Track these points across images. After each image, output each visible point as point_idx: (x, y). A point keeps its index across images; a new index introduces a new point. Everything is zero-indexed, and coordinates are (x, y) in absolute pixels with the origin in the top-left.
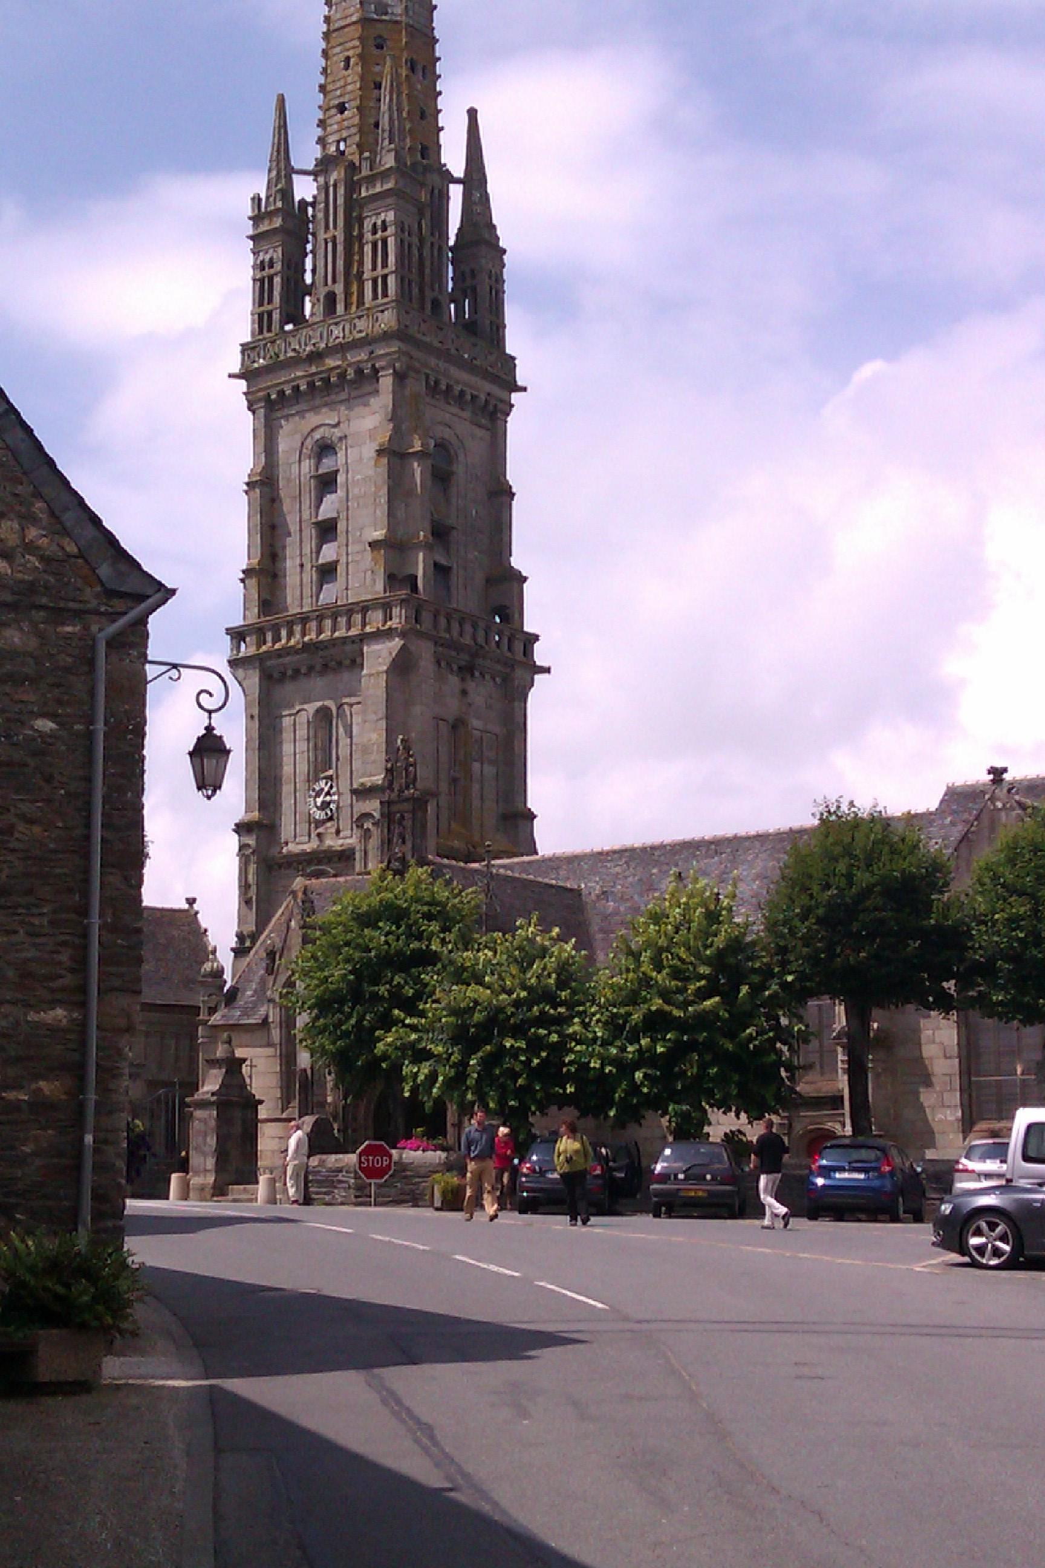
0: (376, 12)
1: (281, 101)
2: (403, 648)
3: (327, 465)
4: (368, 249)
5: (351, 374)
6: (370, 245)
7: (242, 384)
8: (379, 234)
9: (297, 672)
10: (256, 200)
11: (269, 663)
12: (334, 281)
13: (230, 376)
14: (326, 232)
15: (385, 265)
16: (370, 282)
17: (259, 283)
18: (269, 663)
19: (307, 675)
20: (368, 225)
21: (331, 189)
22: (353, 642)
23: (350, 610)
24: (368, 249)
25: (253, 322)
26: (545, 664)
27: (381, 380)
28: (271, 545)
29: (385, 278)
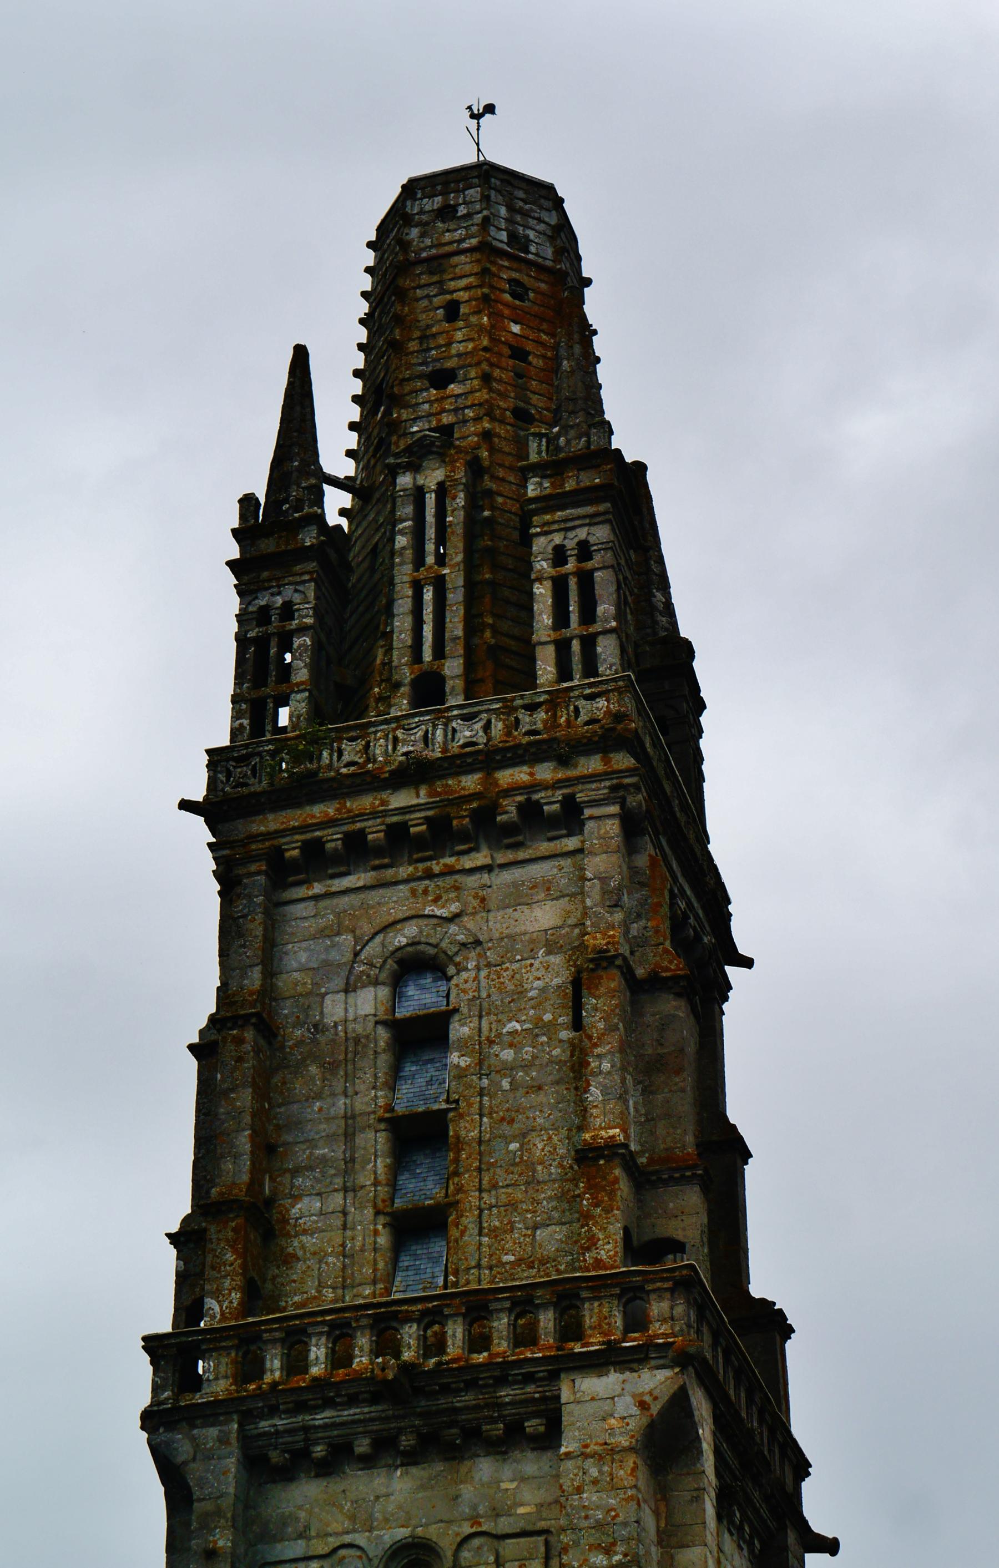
0: (508, 244)
1: (301, 356)
2: (680, 1400)
4: (542, 591)
5: (509, 811)
6: (548, 584)
8: (571, 566)
10: (248, 502)
11: (264, 1425)
12: (439, 652)
13: (185, 805)
14: (416, 569)
15: (588, 615)
16: (551, 650)
19: (368, 1462)
20: (540, 544)
21: (431, 499)
22: (529, 1378)
24: (542, 591)
25: (236, 715)
27: (590, 825)
29: (589, 643)
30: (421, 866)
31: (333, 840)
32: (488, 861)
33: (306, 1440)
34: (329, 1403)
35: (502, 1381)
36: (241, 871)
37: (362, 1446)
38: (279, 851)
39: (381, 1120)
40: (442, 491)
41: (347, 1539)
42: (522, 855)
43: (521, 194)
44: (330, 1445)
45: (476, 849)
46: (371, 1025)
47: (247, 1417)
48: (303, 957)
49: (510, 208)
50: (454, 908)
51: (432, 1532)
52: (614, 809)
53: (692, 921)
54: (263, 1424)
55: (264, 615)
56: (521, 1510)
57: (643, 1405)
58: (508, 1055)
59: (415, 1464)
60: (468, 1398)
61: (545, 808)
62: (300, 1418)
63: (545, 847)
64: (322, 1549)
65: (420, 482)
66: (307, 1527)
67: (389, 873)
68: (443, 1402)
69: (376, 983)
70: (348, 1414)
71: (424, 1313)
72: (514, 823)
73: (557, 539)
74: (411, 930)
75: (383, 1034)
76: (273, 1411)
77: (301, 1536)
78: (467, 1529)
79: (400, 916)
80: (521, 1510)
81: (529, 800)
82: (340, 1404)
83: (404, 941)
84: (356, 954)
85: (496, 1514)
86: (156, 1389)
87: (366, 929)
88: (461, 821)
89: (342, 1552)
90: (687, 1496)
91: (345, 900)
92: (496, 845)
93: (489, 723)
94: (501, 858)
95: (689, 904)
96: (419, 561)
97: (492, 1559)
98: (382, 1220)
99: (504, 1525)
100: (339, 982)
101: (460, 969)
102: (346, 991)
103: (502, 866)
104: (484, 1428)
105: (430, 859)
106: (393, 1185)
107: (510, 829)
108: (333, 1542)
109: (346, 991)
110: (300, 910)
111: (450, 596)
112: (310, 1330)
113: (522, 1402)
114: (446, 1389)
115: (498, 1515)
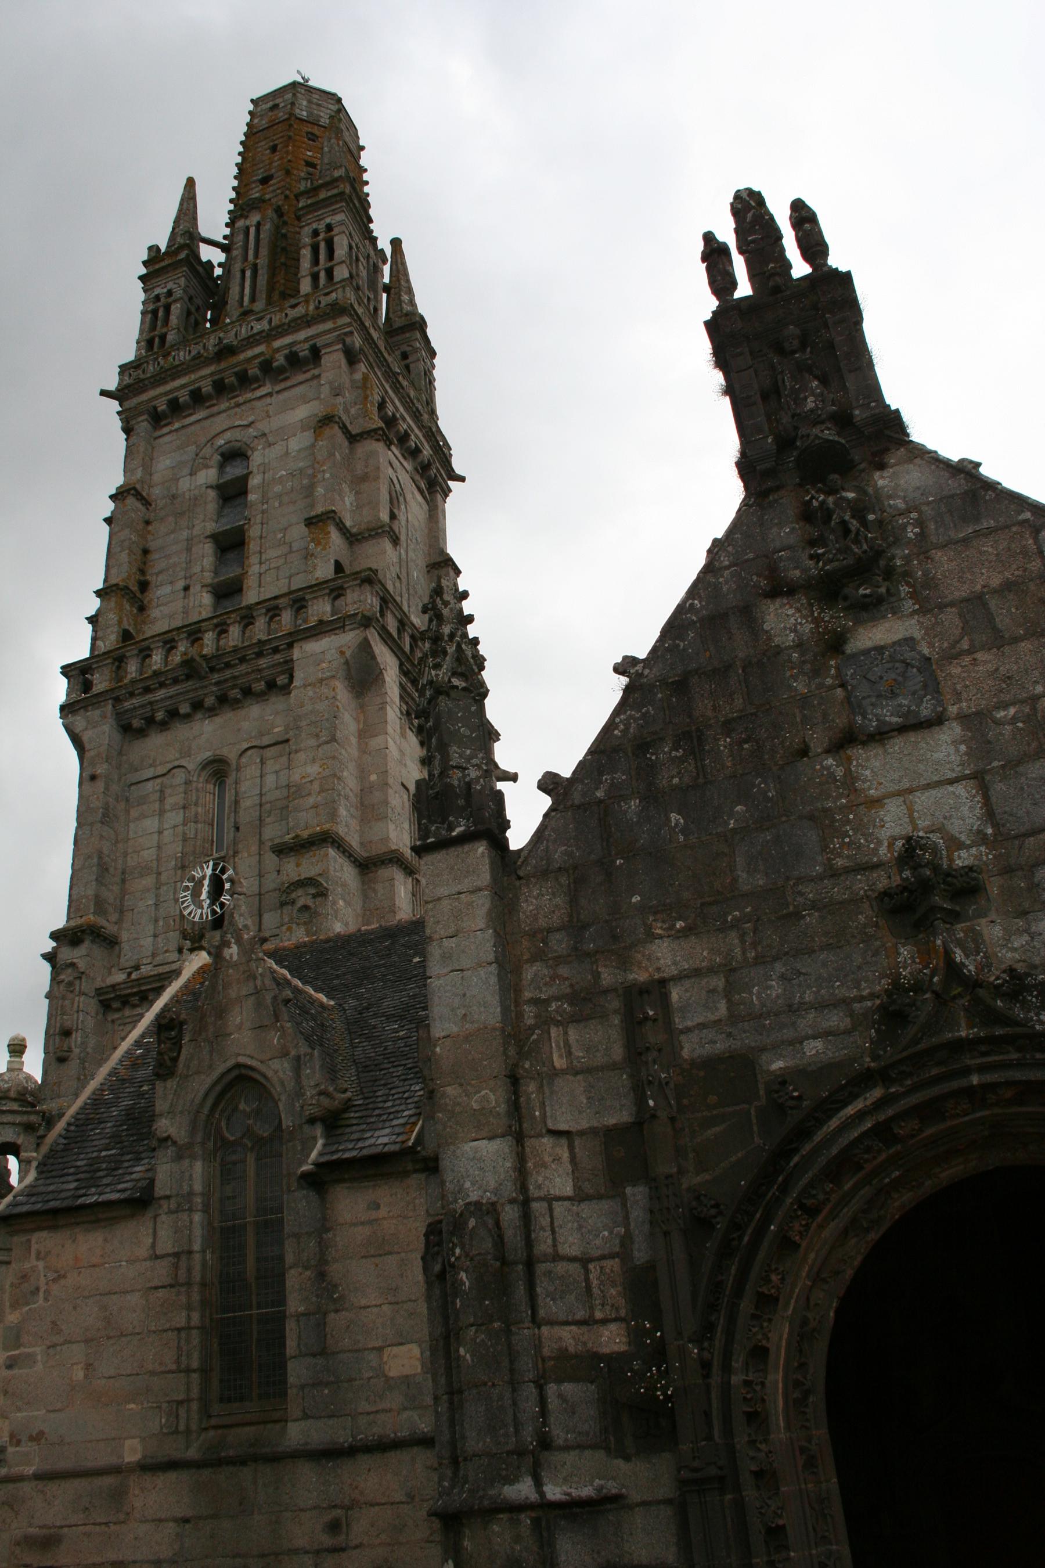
1: (190, 183)
3: (234, 471)
6: (309, 248)
7: (115, 405)
8: (322, 236)
9: (173, 714)
10: (154, 249)
11: (127, 705)
12: (253, 299)
13: (104, 393)
17: (150, 316)
18: (127, 705)
19: (187, 717)
21: (252, 230)
22: (276, 650)
23: (272, 609)
26: (512, 770)
28: (142, 572)
30: (233, 401)
31: (184, 397)
32: (270, 390)
33: (152, 710)
34: (162, 685)
35: (260, 655)
36: (134, 422)
37: (185, 709)
38: (155, 408)
39: (207, 537)
40: (258, 226)
41: (176, 763)
42: (289, 383)
43: (317, 97)
44: (167, 711)
45: (264, 385)
46: (204, 489)
47: (117, 700)
48: (168, 462)
49: (310, 102)
50: (251, 419)
51: (225, 752)
52: (340, 346)
53: (413, 437)
54: (126, 704)
55: (157, 298)
56: (276, 730)
57: (342, 653)
58: (278, 489)
59: (216, 715)
60: (243, 668)
61: (301, 354)
62: (147, 697)
63: (301, 377)
64: (161, 770)
65: (248, 222)
66: (155, 761)
67: (215, 409)
68: (228, 673)
69: (207, 467)
70: (173, 690)
71: (216, 626)
72: (282, 366)
73: (315, 226)
74: (228, 435)
75: (212, 494)
76: (132, 695)
77: (151, 766)
78: (245, 746)
79: (222, 429)
80: (276, 730)
81: (291, 352)
82: (170, 685)
83: (223, 442)
84: (197, 455)
85: (261, 734)
86: (68, 694)
87: (204, 440)
88: (254, 371)
89: (174, 771)
90: (377, 708)
91: (193, 428)
92: (276, 381)
93: (271, 319)
94: (277, 388)
95: (409, 426)
96: (245, 258)
97: (258, 760)
98: (205, 589)
99: (266, 740)
100: (186, 471)
101: (253, 450)
102: (191, 475)
103: (278, 392)
104: (253, 686)
105: (237, 396)
106: (216, 573)
107: (281, 370)
108: (169, 766)
109: (191, 475)
110: (167, 439)
111: (260, 272)
112: (152, 646)
113: (273, 666)
114: (228, 665)
115: (263, 735)
